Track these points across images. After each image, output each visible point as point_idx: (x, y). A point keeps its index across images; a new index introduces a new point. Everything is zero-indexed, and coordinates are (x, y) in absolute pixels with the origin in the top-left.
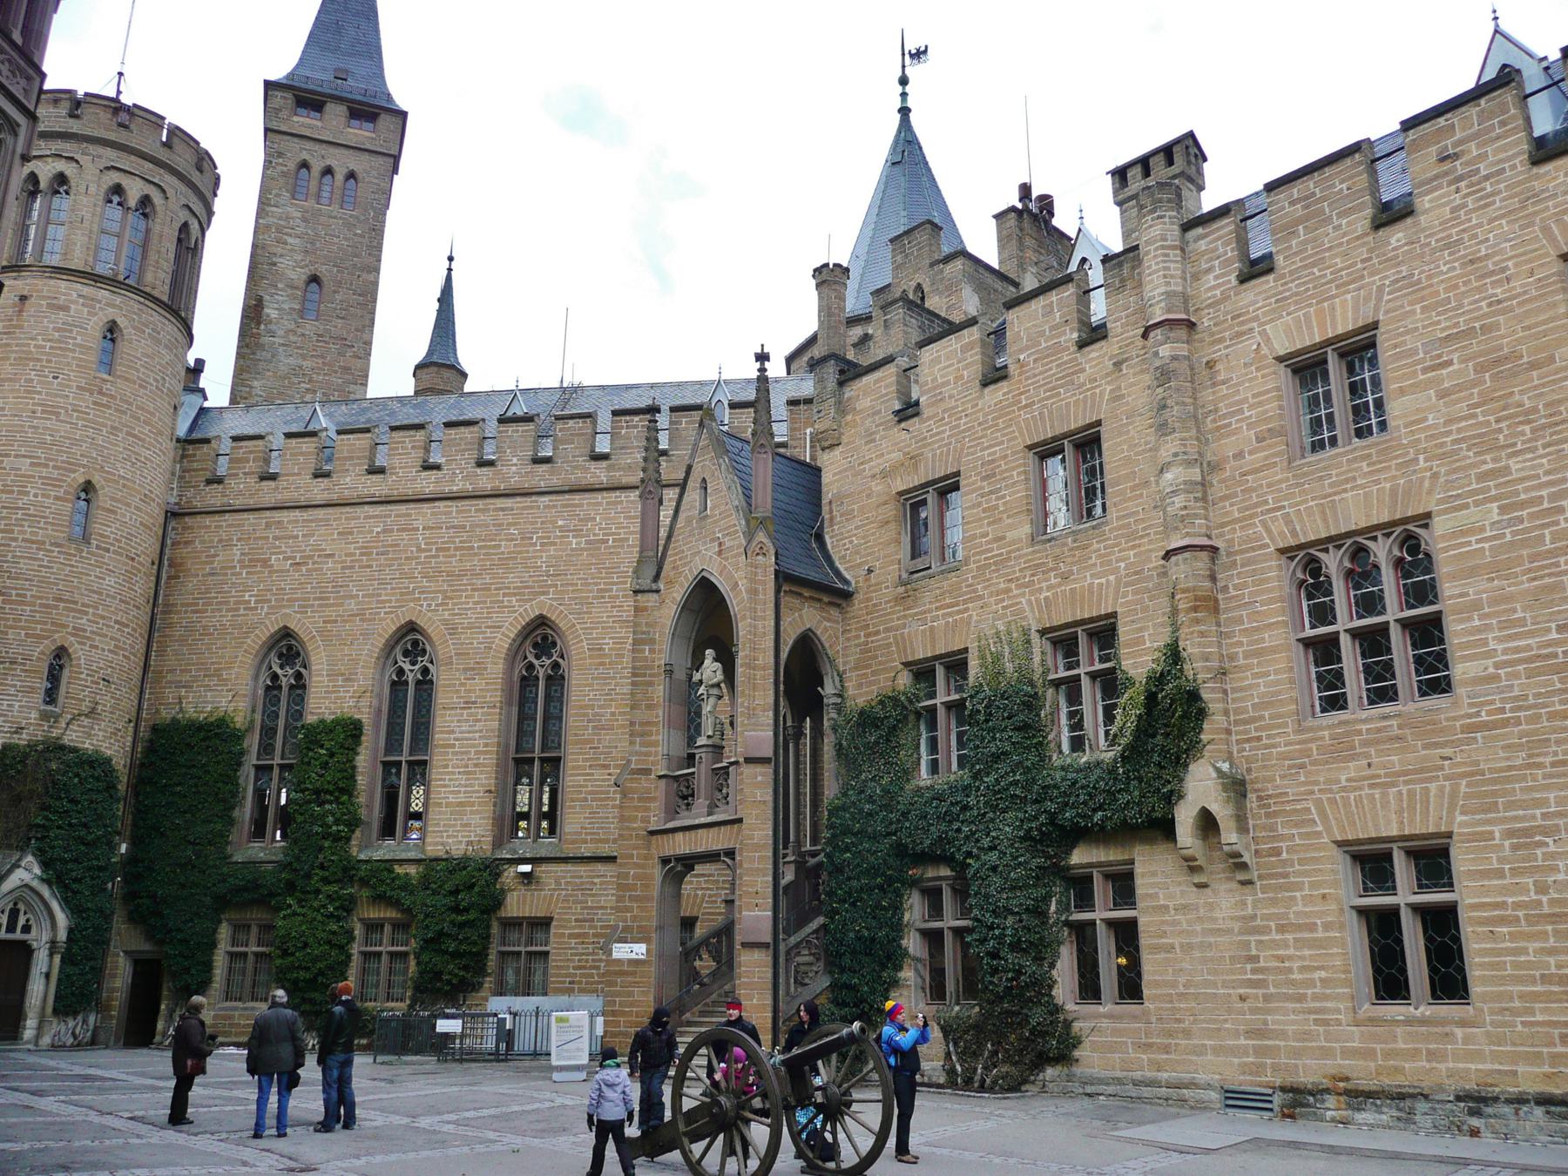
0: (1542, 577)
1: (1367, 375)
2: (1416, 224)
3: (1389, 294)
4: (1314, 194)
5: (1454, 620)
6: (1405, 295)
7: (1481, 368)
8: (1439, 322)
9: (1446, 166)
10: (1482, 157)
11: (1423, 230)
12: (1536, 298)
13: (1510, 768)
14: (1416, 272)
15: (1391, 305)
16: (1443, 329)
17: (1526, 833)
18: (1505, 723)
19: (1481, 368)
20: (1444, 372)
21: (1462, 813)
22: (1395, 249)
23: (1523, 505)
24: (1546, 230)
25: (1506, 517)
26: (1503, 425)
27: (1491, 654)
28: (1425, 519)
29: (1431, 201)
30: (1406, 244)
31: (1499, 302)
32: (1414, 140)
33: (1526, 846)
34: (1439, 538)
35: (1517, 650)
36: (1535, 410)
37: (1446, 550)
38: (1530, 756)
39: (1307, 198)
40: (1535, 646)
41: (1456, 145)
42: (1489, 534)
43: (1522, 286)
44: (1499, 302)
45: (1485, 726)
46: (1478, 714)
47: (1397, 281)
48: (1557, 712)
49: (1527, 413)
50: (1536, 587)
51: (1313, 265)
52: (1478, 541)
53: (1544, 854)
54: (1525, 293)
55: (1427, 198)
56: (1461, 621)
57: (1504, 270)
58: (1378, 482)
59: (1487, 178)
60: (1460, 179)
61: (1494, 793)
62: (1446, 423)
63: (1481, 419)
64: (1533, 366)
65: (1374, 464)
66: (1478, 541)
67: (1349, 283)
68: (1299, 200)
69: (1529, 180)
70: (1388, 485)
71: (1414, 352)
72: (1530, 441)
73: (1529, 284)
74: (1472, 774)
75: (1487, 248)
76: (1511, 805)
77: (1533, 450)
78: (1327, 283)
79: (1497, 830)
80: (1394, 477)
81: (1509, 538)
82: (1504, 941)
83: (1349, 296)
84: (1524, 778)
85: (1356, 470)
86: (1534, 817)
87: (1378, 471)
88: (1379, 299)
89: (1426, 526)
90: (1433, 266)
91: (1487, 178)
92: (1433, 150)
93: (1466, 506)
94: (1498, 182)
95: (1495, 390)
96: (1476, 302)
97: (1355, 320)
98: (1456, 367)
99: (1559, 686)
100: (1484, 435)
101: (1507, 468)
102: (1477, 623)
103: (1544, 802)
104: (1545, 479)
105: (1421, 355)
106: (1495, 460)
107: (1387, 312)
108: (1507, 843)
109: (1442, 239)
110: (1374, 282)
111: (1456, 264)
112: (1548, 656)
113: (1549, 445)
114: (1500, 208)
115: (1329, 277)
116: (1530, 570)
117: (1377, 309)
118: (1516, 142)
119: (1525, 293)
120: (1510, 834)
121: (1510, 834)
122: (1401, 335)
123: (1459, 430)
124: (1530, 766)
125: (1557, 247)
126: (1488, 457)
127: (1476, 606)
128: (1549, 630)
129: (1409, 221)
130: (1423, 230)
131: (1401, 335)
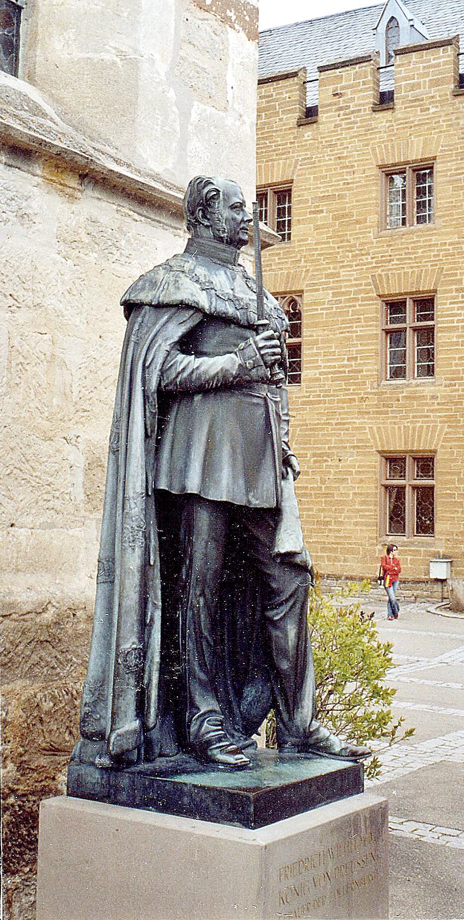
0: (345, 333)
1: (287, 206)
2: (318, 128)
3: (301, 165)
4: (272, 95)
5: (306, 348)
6: (308, 168)
7: (335, 218)
8: (320, 188)
9: (336, 99)
10: (353, 99)
11: (321, 134)
12: (364, 186)
13: (318, 424)
14: (314, 157)
15: (300, 172)
16: (322, 192)
17: (320, 455)
18: (319, 402)
19: (335, 218)
20: (319, 216)
21: (296, 444)
22: (306, 141)
23: (343, 294)
24: (374, 149)
25: (334, 299)
26: (340, 250)
27: (319, 367)
28: (300, 293)
29: (326, 118)
30: (312, 139)
31: (348, 184)
32: (323, 79)
33: (320, 462)
34: (305, 305)
35: (329, 367)
36: (355, 245)
37: (307, 311)
38: (327, 419)
39: (268, 96)
40: (337, 366)
41: (342, 88)
42: (326, 306)
43: (359, 177)
44: (348, 184)
45: (311, 403)
46: (309, 397)
47: (305, 159)
48: (341, 399)
49: (351, 246)
50: (343, 337)
51: (266, 138)
52: (322, 309)
53: (326, 465)
54: (359, 182)
55: (325, 115)
56: (309, 349)
57: (353, 166)
58: (281, 269)
59: (353, 112)
60: (341, 109)
61: (310, 436)
62: (316, 244)
63: (331, 245)
64: (358, 222)
65: (282, 258)
66: (322, 309)
67: (283, 154)
68: (265, 97)
69: (370, 119)
70: (286, 272)
71: (307, 201)
72: (350, 261)
73: (362, 177)
74: (303, 425)
75: (347, 152)
76: (315, 442)
77: (351, 266)
78: (272, 151)
79: (309, 453)
80: (289, 268)
81: (334, 310)
82: (305, 504)
83: (281, 162)
84: (323, 429)
85: (272, 260)
86: (324, 448)
87: (282, 263)
88: (295, 167)
89: (301, 296)
90: (321, 155)
91: (353, 112)
92: (331, 87)
93: (318, 290)
94: (357, 117)
95: (339, 232)
96: (338, 181)
97: (283, 176)
98: (324, 214)
99: (344, 387)
100: (330, 254)
101: (339, 273)
102: (315, 351)
103: (329, 441)
104: (354, 282)
105: (310, 204)
106: (334, 268)
107: (298, 176)
108: (312, 460)
109: (328, 141)
110: (293, 157)
111: (332, 157)
112: (341, 372)
113: (358, 265)
114: (356, 132)
115: (274, 148)
116: (340, 328)
117: (293, 173)
118: (367, 97)
119: (359, 182)
120: (314, 455)
121: (314, 455)
122: (302, 190)
123: (322, 249)
124: (327, 424)
125: (377, 161)
126: (331, 266)
127: (316, 342)
128: (344, 359)
129: (315, 125)
130: (321, 134)
131: (302, 190)
